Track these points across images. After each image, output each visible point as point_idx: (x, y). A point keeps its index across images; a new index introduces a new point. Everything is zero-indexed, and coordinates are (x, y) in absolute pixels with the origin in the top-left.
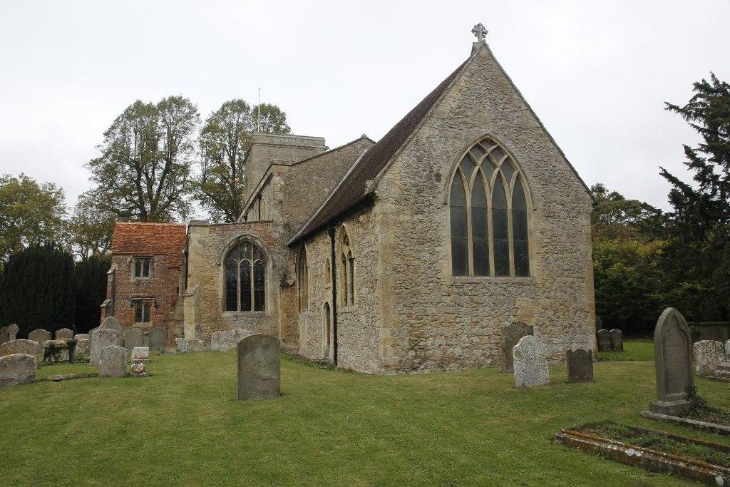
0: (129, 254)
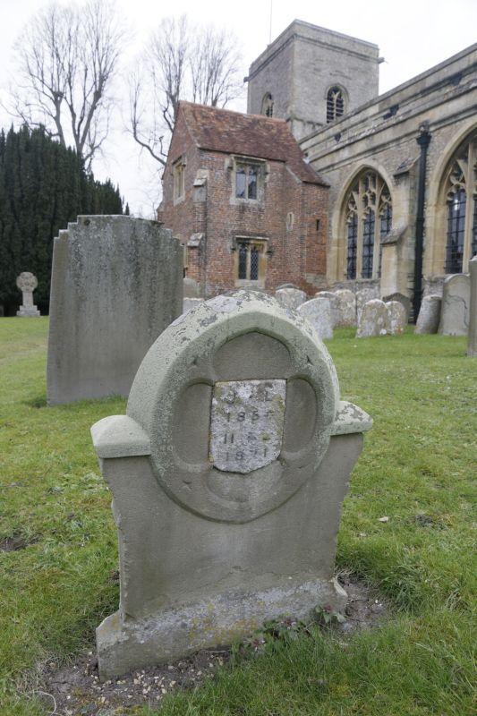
0: (229, 153)
